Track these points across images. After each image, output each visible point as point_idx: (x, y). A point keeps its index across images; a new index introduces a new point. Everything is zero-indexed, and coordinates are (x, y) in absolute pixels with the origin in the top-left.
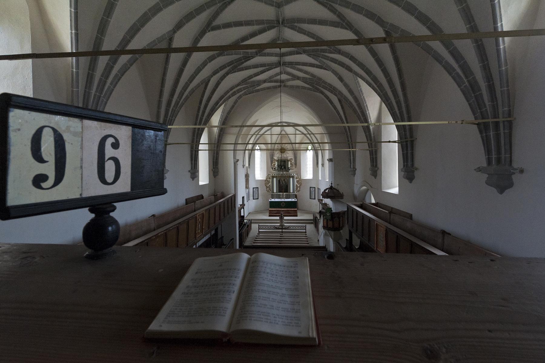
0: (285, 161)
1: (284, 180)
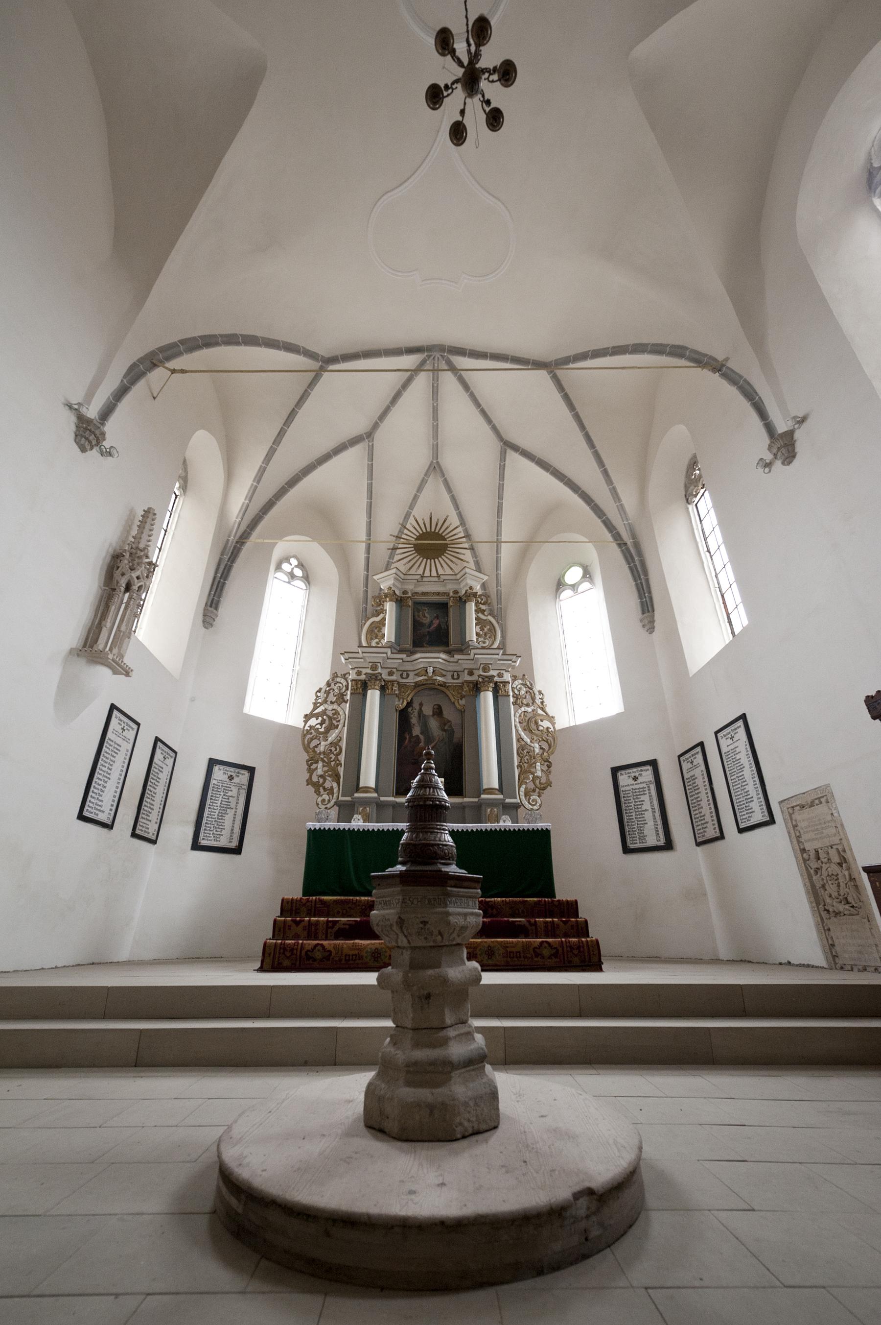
0: (442, 607)
1: (438, 712)
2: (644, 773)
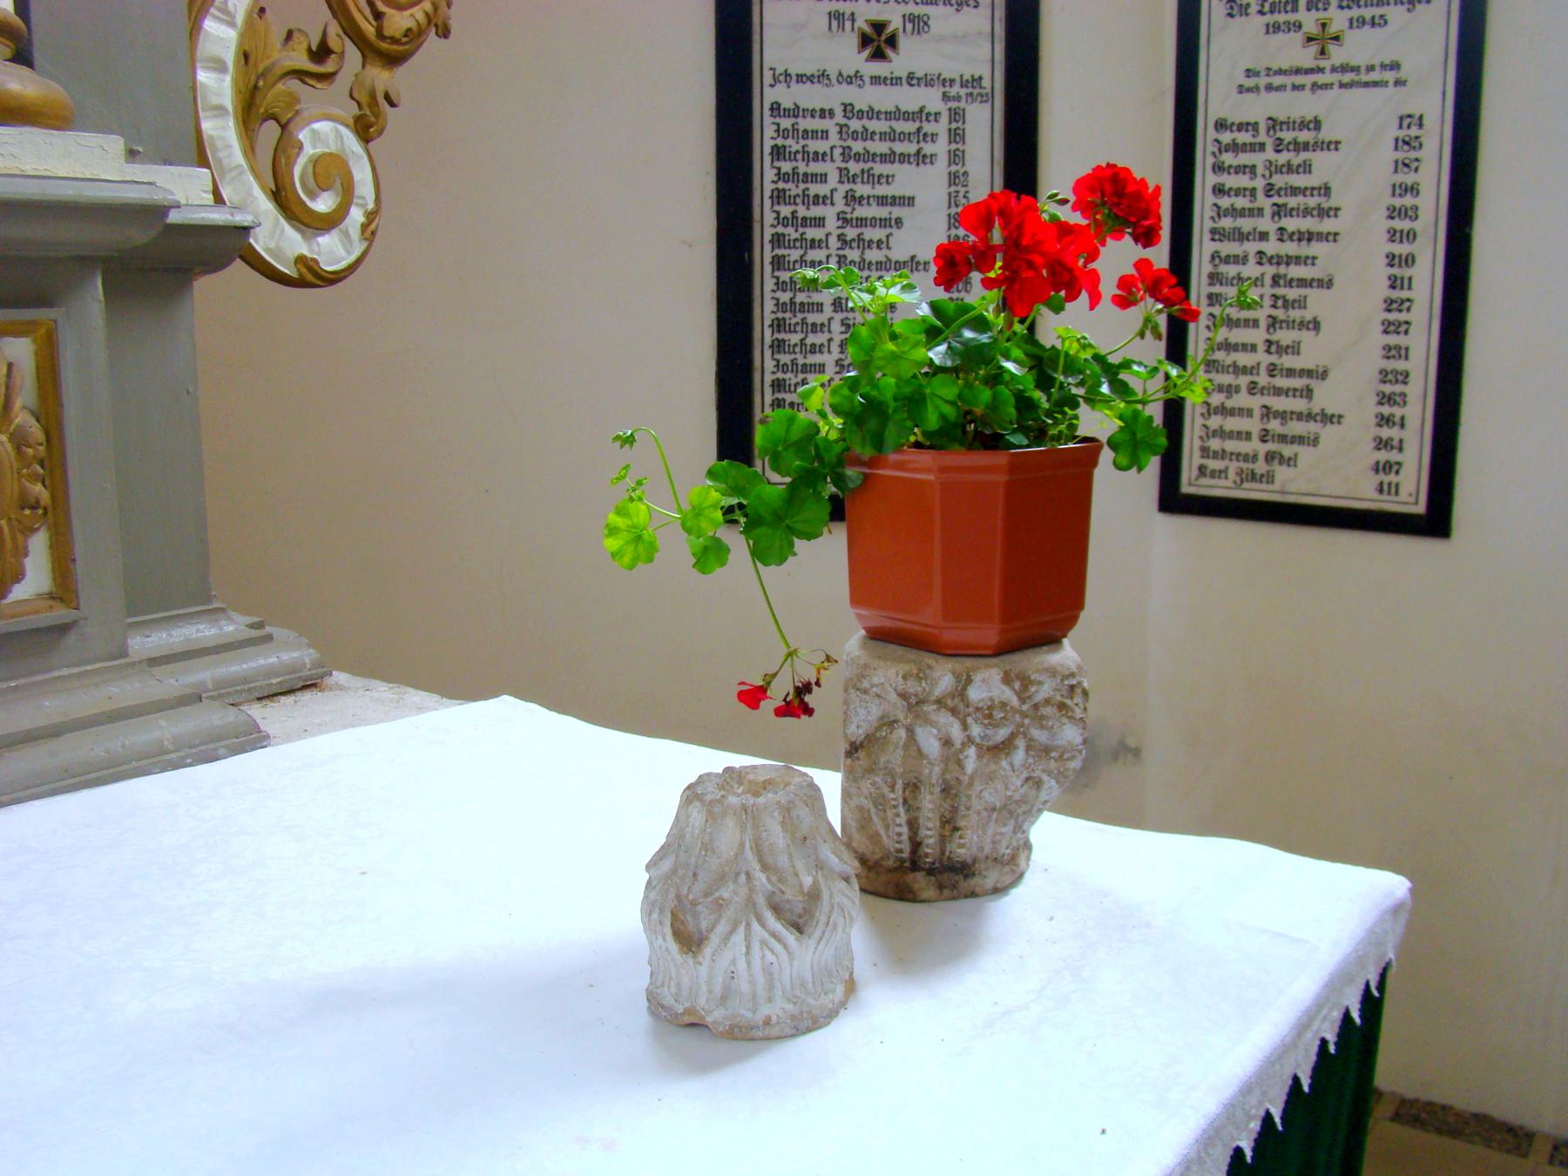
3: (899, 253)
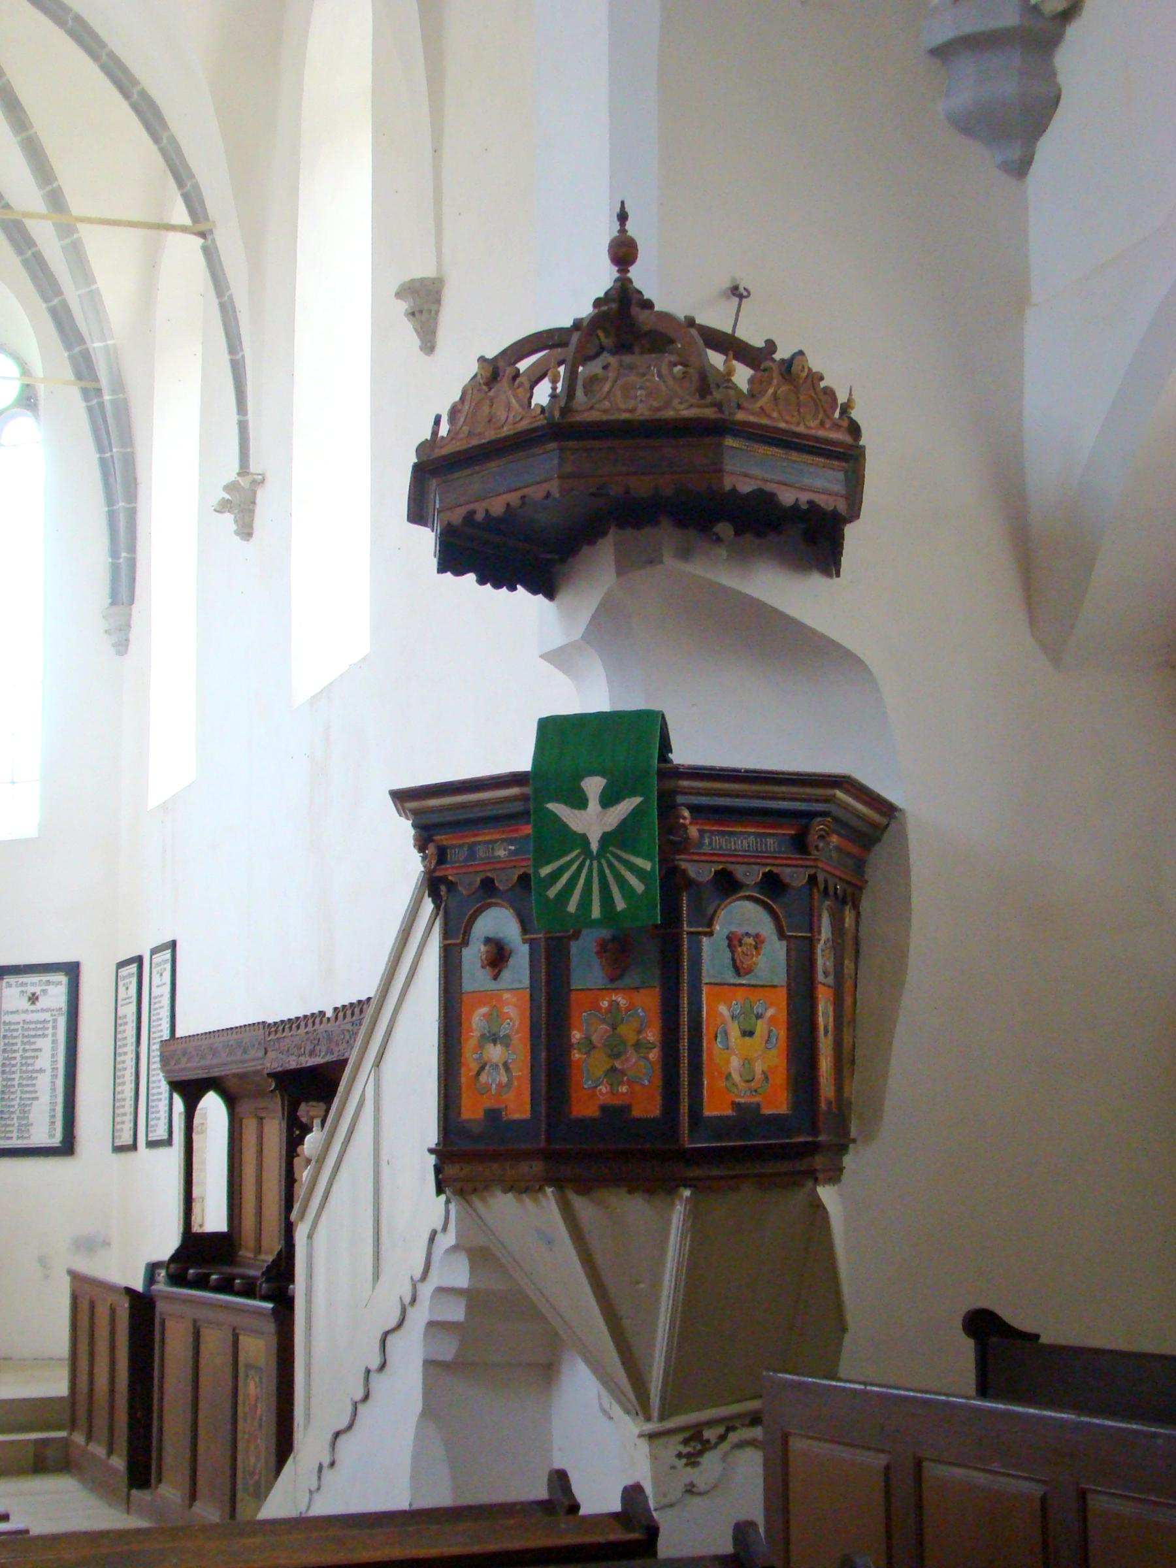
2: (52, 989)
3: (37, 1067)
